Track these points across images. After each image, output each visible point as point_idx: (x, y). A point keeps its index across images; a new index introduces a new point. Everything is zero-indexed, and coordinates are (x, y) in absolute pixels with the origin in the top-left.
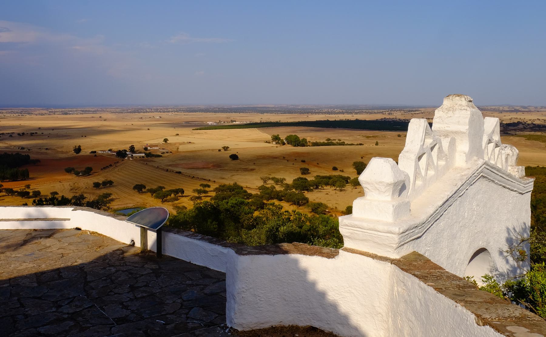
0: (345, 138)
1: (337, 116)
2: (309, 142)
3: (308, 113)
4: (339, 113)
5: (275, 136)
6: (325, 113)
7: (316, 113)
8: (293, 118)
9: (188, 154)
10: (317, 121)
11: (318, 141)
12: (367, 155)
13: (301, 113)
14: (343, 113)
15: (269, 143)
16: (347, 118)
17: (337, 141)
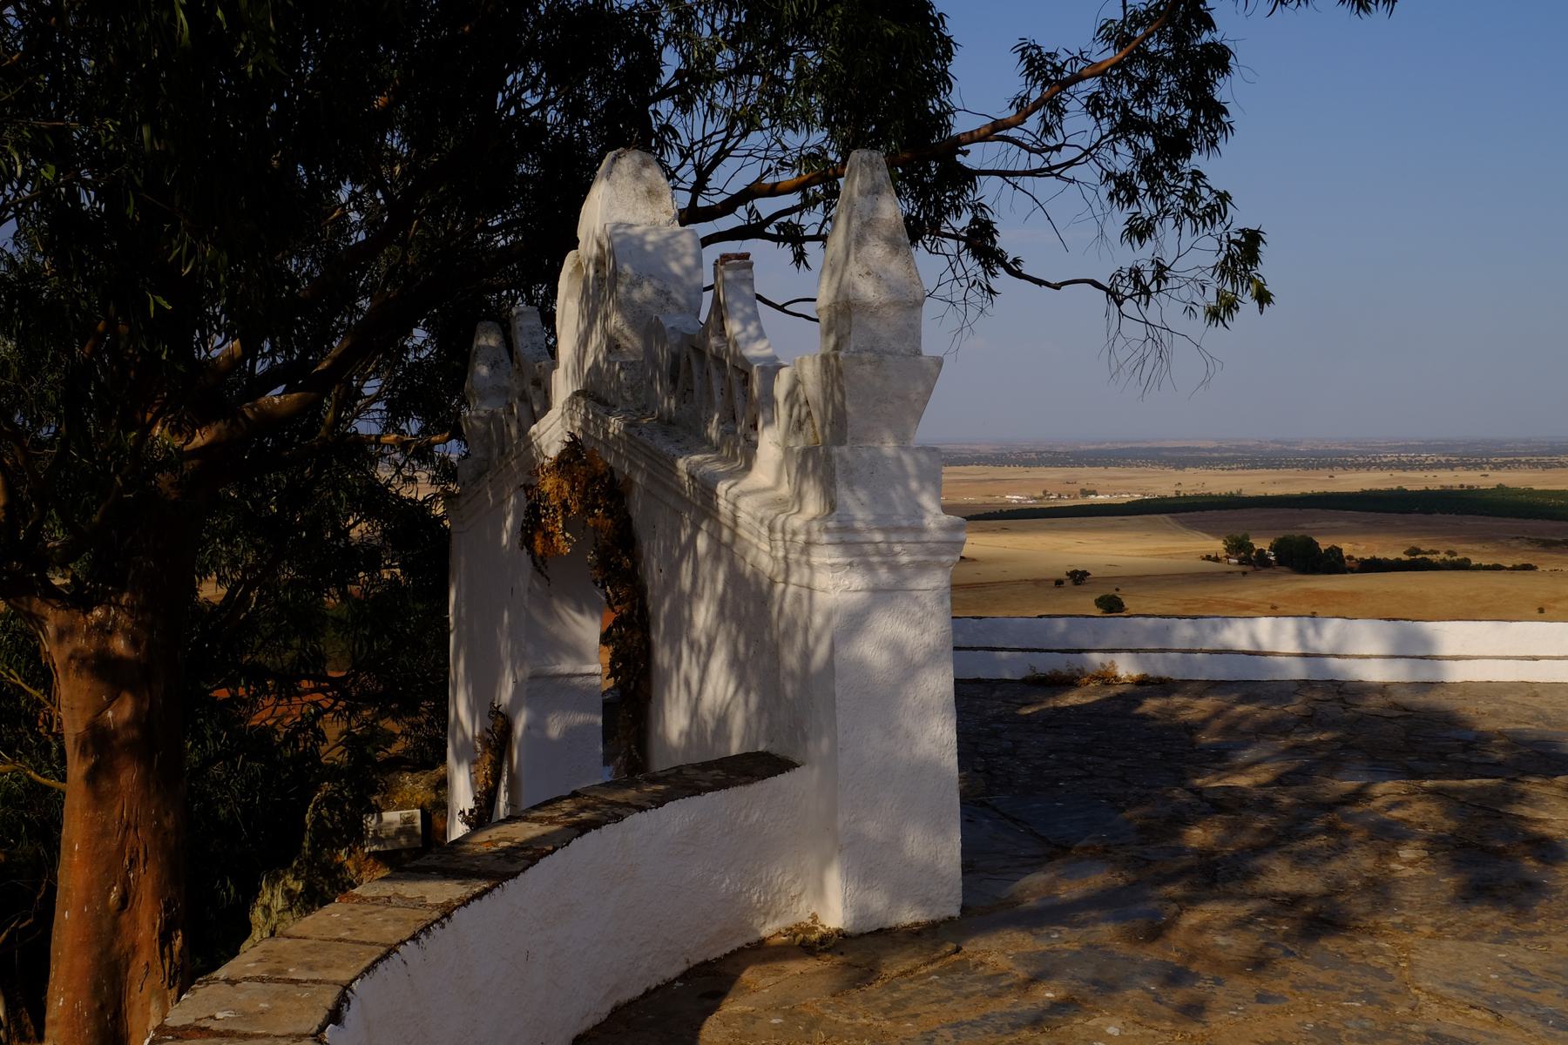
0: (1469, 547)
1: (1430, 475)
2: (1350, 558)
3: (1331, 466)
4: (1437, 466)
5: (1237, 540)
6: (1389, 466)
7: (1358, 466)
8: (1284, 481)
9: (653, 707)
10: (1364, 492)
11: (1380, 556)
12: (1556, 600)
13: (1307, 466)
14: (1450, 466)
15: (1217, 559)
16: (1466, 483)
17: (1442, 556)
